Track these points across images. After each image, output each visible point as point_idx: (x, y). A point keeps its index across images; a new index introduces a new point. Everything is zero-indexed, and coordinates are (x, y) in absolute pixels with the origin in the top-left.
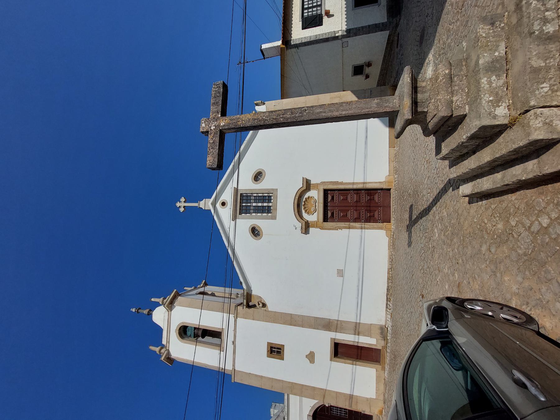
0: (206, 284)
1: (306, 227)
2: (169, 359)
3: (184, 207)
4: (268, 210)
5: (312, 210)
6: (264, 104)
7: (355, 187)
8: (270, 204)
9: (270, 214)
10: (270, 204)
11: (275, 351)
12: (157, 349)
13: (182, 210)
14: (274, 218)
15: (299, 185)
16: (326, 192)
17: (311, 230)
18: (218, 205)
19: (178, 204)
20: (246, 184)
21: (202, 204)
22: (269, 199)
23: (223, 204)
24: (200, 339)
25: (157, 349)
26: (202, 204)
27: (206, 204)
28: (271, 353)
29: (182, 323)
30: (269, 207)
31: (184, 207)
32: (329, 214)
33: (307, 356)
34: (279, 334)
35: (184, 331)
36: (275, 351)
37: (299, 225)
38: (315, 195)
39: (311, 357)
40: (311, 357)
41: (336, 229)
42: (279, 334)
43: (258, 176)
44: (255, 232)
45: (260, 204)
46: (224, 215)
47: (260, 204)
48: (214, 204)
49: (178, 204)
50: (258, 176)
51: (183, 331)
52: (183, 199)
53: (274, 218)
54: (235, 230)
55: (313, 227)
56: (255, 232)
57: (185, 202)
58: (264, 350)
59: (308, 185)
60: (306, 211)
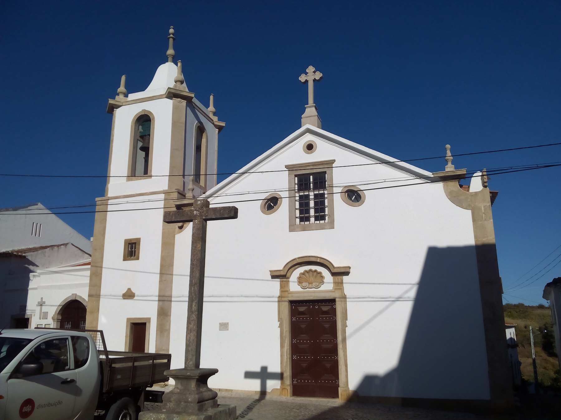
0: (220, 128)
1: (281, 276)
2: (112, 109)
3: (307, 81)
4: (304, 218)
5: (304, 284)
6: (485, 187)
7: (340, 346)
8: (312, 219)
9: (298, 220)
10: (312, 219)
11: (132, 249)
12: (122, 89)
13: (302, 78)
14: (292, 228)
15: (338, 263)
16: (333, 301)
17: (277, 283)
18: (308, 138)
19: (311, 69)
20: (340, 179)
21: (311, 111)
22: (320, 217)
23: (310, 147)
24: (140, 144)
25: (122, 89)
26: (311, 111)
27: (310, 116)
28: (129, 244)
29: (154, 118)
30: (308, 219)
31: (307, 81)
32: (302, 309)
33: (129, 289)
34: (151, 252)
35: (144, 122)
36: (132, 249)
37: (279, 266)
38: (327, 287)
39: (129, 295)
40: (129, 295)
41: (280, 319)
42: (151, 252)
43: (353, 195)
44: (271, 203)
45: (312, 204)
46: (292, 152)
47: (312, 204)
48: (309, 131)
49: (311, 69)
50: (353, 195)
51: (144, 122)
52: (318, 75)
53: (292, 228)
54: (272, 171)
55: (281, 287)
56: (271, 203)
57: (315, 80)
58: (132, 236)
59: (340, 274)
60: (303, 274)
